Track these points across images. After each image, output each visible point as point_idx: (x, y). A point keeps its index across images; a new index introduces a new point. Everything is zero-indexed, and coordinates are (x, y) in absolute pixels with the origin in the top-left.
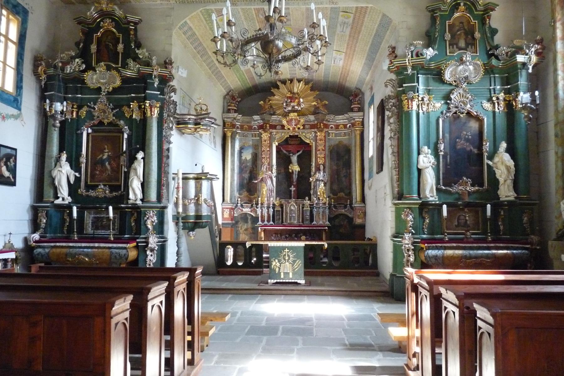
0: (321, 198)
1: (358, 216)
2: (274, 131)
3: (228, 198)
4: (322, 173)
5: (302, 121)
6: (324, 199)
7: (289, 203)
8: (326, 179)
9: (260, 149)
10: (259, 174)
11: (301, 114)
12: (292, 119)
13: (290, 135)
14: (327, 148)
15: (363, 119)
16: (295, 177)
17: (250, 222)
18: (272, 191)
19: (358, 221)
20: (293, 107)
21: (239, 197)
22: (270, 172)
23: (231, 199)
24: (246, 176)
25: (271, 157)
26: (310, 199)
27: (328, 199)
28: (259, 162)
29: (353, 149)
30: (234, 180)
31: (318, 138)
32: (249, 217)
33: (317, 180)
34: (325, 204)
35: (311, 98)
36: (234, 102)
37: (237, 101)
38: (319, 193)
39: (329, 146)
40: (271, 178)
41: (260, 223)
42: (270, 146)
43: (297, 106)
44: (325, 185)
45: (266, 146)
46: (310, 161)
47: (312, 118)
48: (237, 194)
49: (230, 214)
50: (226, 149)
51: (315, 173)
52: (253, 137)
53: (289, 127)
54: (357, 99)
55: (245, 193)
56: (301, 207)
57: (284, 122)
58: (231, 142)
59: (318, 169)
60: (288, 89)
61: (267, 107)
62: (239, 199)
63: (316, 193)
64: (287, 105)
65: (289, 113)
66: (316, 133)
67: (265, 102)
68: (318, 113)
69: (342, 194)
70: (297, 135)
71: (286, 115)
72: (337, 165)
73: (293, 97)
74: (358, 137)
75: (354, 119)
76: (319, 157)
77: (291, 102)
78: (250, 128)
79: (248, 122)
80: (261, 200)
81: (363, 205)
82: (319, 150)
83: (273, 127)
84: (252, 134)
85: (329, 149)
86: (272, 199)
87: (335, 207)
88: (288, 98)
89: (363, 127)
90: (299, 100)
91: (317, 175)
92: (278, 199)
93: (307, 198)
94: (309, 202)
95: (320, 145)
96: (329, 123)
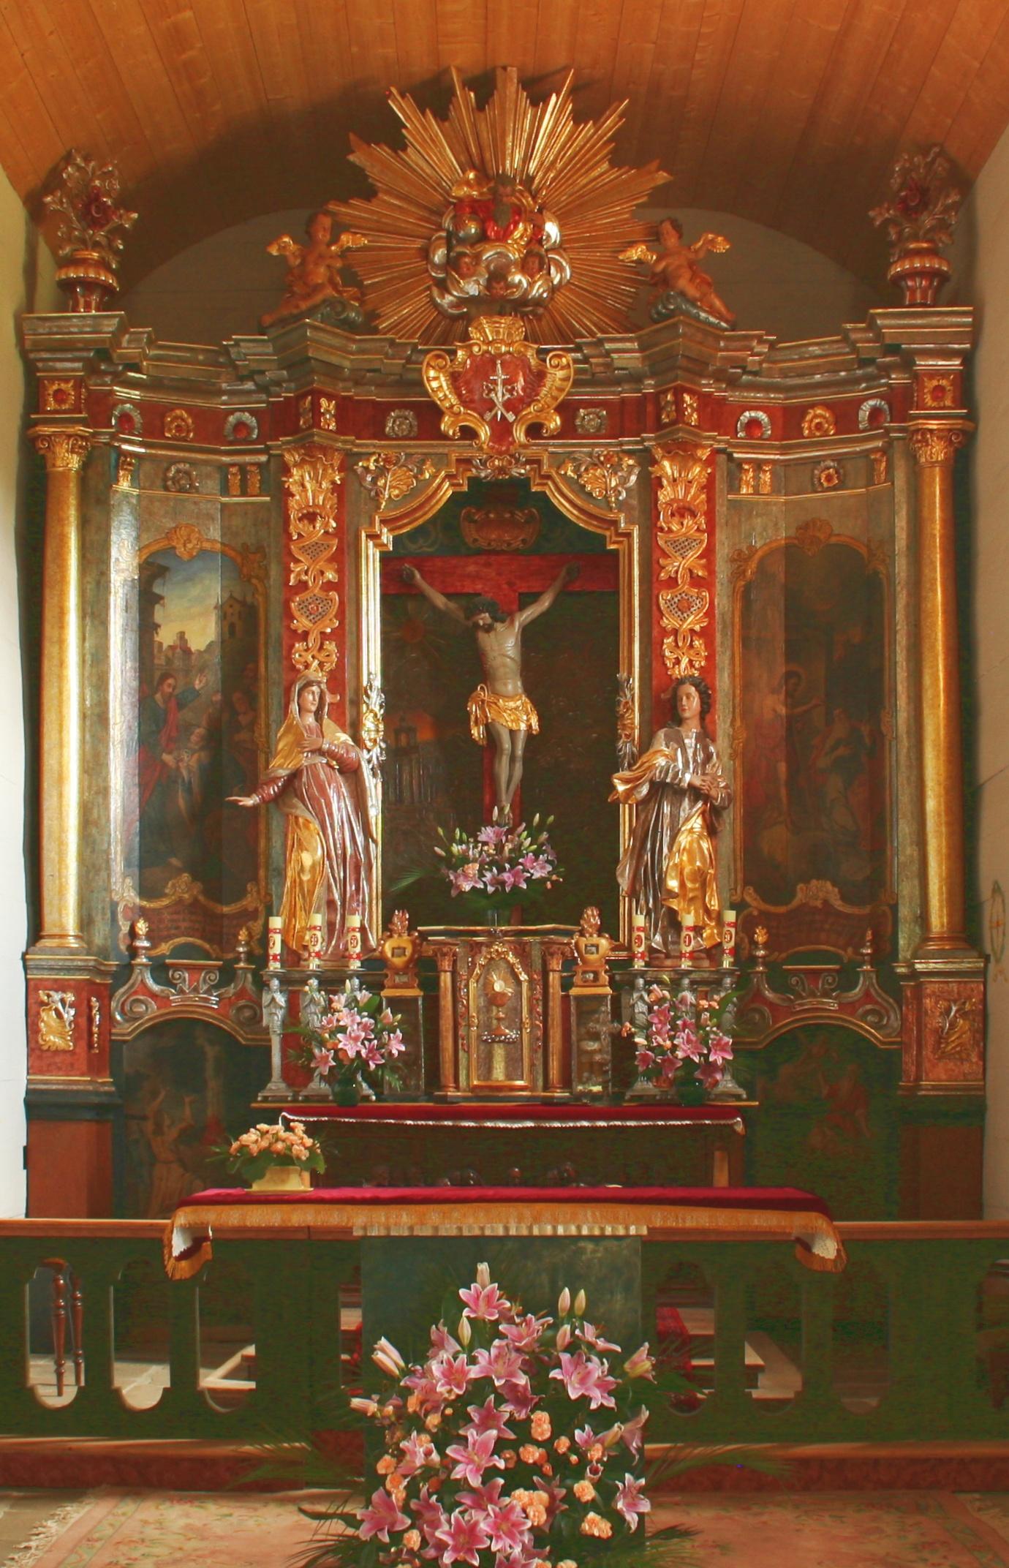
0: (689, 920)
1: (940, 1036)
2: (369, 444)
3: (65, 912)
4: (690, 742)
5: (558, 374)
6: (708, 922)
7: (475, 949)
8: (721, 778)
9: (274, 571)
10: (270, 754)
11: (543, 322)
12: (485, 365)
13: (474, 481)
14: (723, 571)
15: (968, 359)
16: (508, 773)
17: (214, 1085)
18: (359, 867)
19: (937, 1077)
20: (498, 276)
21: (143, 913)
22: (344, 737)
23: (85, 923)
24: (187, 761)
25: (347, 636)
26: (609, 926)
27: (730, 916)
28: (269, 668)
29: (901, 567)
30: (104, 792)
31: (665, 495)
32: (211, 1051)
33: (664, 789)
34: (713, 953)
35: (620, 211)
36: (101, 235)
37: (120, 231)
38: (673, 884)
39: (739, 559)
40: (351, 772)
41: (276, 1085)
42: (346, 557)
43: (524, 267)
44: (711, 830)
45: (314, 550)
46: (610, 660)
47: (626, 353)
48: (124, 890)
49: (82, 1028)
50: (51, 569)
51: (646, 744)
52: (225, 490)
53: (471, 420)
54: (927, 221)
55: (181, 887)
56: (554, 979)
57: (437, 383)
58: (84, 524)
59: (664, 712)
60: (460, 145)
61: (320, 274)
62: (142, 927)
63: (650, 879)
64: (452, 263)
65: (468, 319)
66: (646, 459)
67: (307, 238)
68: (672, 314)
69: (821, 892)
70: (524, 483)
71: (448, 331)
72: (793, 689)
73: (497, 205)
74: (936, 489)
75: (907, 362)
76: (684, 626)
77: (483, 238)
78: (210, 428)
79: (188, 387)
80: (285, 932)
81: (968, 963)
82: (672, 582)
83: (363, 420)
84: (223, 469)
85: (737, 574)
86: (355, 921)
87: (778, 979)
88: (463, 208)
89: (972, 417)
90: (539, 229)
91: (662, 758)
92: (400, 919)
93: (592, 916)
94: (604, 943)
95: (681, 546)
96: (734, 396)
